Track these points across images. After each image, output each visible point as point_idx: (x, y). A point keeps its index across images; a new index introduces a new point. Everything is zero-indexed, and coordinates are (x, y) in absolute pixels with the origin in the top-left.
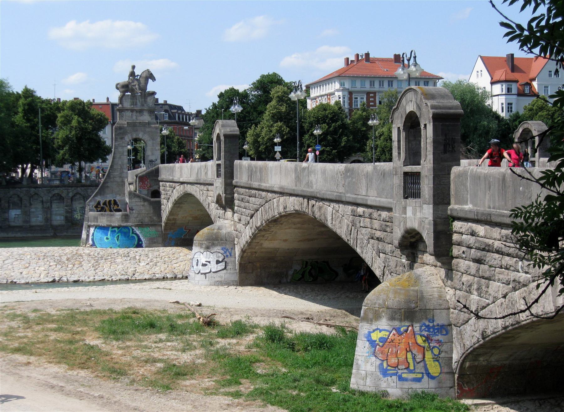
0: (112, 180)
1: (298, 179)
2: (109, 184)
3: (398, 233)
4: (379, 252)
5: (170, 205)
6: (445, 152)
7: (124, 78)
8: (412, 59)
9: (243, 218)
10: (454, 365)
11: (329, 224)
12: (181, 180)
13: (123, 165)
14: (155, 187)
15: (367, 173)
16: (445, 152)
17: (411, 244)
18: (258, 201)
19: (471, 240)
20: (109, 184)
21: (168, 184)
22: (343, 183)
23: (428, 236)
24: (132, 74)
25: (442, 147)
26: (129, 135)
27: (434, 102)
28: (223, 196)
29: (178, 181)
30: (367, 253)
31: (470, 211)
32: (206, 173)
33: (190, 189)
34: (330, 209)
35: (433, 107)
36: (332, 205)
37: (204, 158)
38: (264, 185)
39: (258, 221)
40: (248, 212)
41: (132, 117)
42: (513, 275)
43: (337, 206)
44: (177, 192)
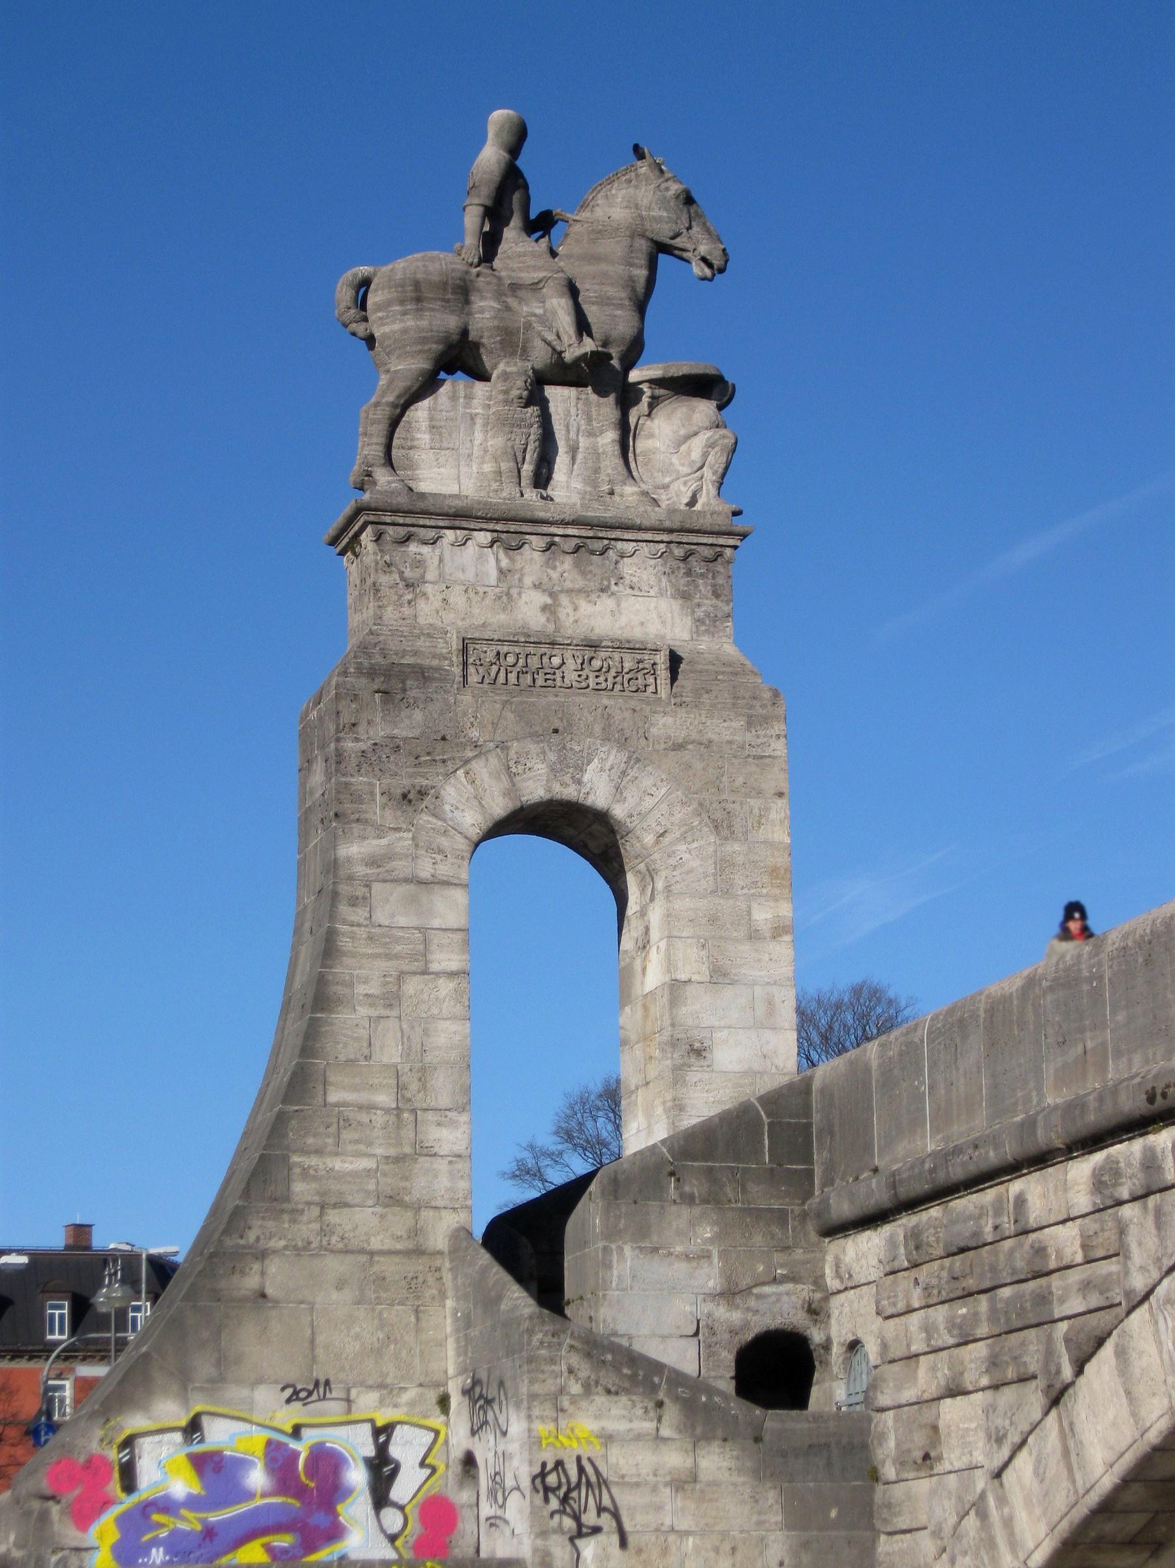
0: (306, 1228)
2: (276, 1276)
13: (424, 1074)
20: (276, 1276)
26: (483, 770)
41: (506, 599)
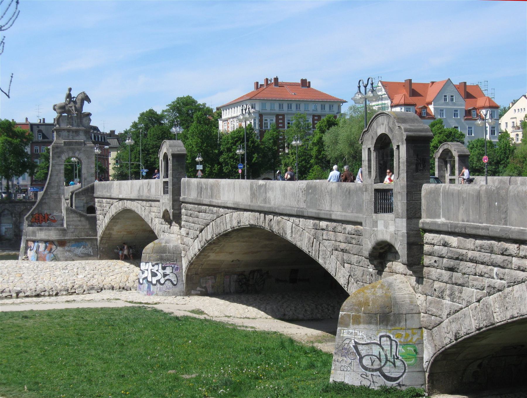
1: (253, 195)
3: (368, 245)
4: (343, 263)
5: (107, 220)
6: (417, 170)
7: (62, 100)
8: (369, 87)
9: (191, 232)
10: (425, 365)
11: (289, 237)
12: (121, 196)
13: (60, 181)
14: (92, 204)
15: (331, 190)
16: (417, 170)
17: (382, 254)
18: (209, 217)
19: (444, 250)
20: (47, 201)
21: (104, 200)
22: (305, 199)
23: (401, 247)
24: (69, 96)
25: (414, 167)
26: (66, 154)
27: (408, 126)
28: (171, 211)
29: (117, 197)
30: (330, 264)
31: (444, 224)
32: (149, 190)
33: (129, 205)
34: (289, 224)
35: (406, 130)
36: (292, 219)
37: (150, 175)
38: (215, 201)
39: (209, 234)
40: (197, 226)
41: (68, 137)
42: (486, 281)
43: (297, 220)
44: (116, 208)
